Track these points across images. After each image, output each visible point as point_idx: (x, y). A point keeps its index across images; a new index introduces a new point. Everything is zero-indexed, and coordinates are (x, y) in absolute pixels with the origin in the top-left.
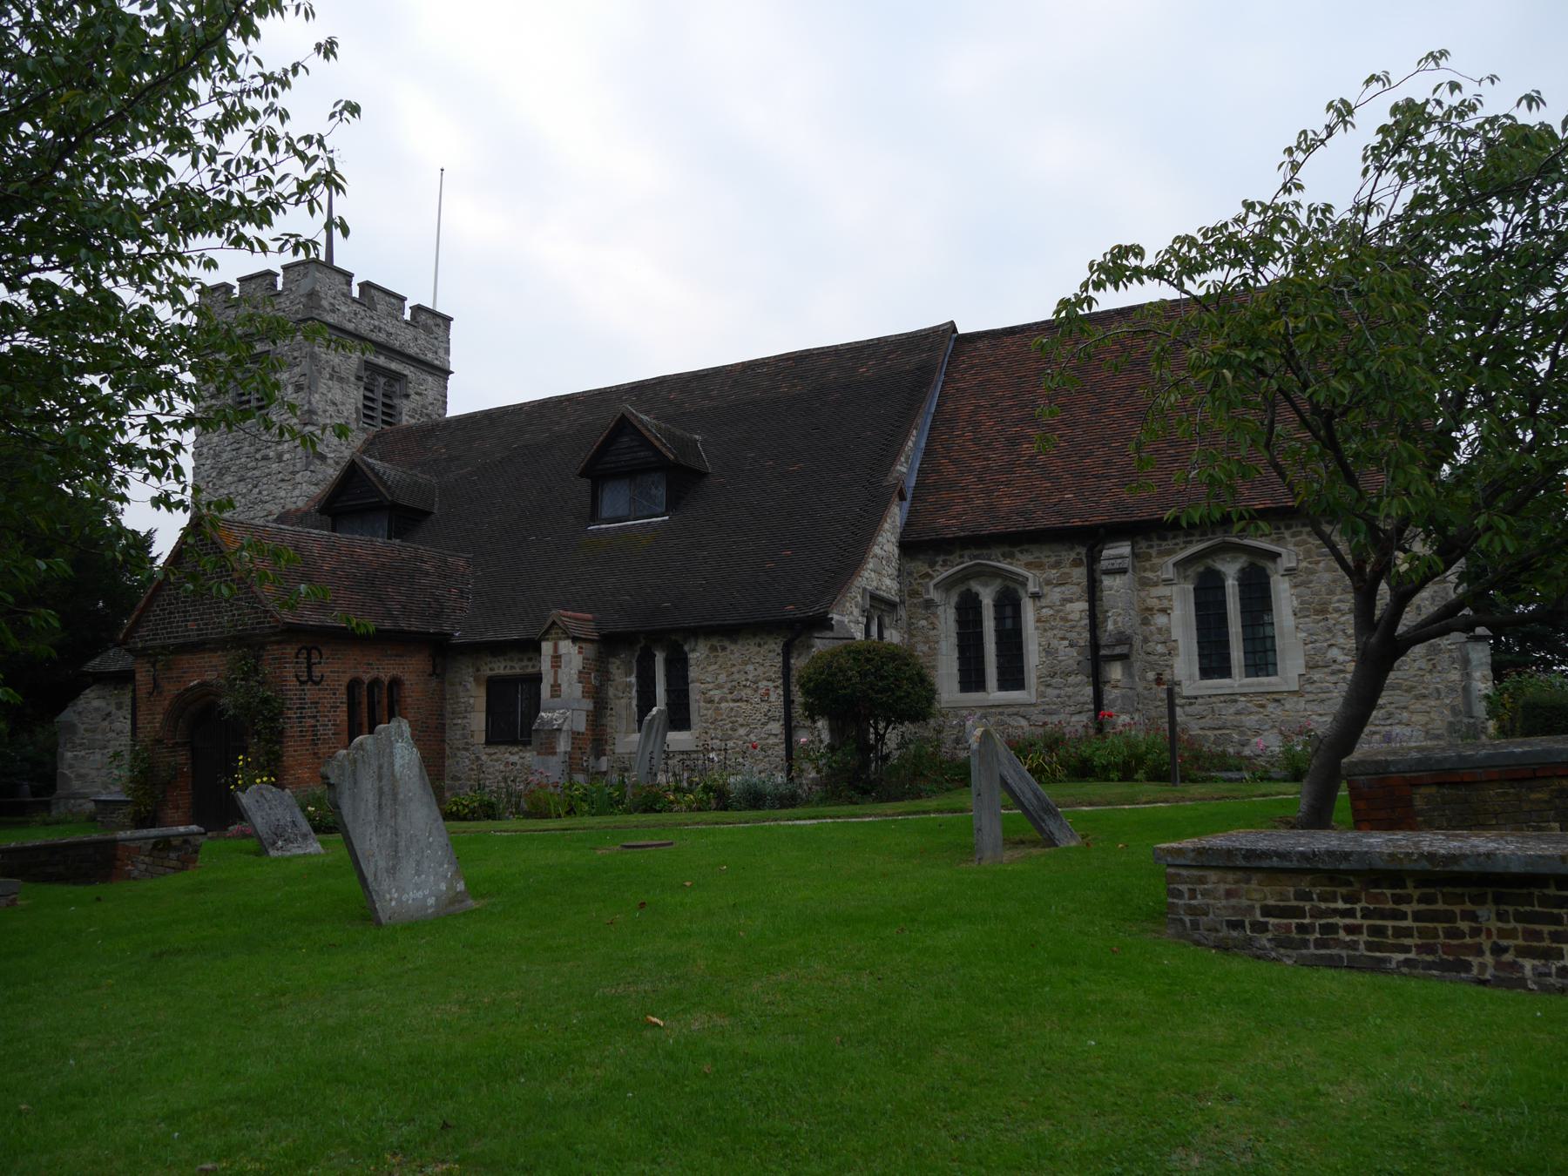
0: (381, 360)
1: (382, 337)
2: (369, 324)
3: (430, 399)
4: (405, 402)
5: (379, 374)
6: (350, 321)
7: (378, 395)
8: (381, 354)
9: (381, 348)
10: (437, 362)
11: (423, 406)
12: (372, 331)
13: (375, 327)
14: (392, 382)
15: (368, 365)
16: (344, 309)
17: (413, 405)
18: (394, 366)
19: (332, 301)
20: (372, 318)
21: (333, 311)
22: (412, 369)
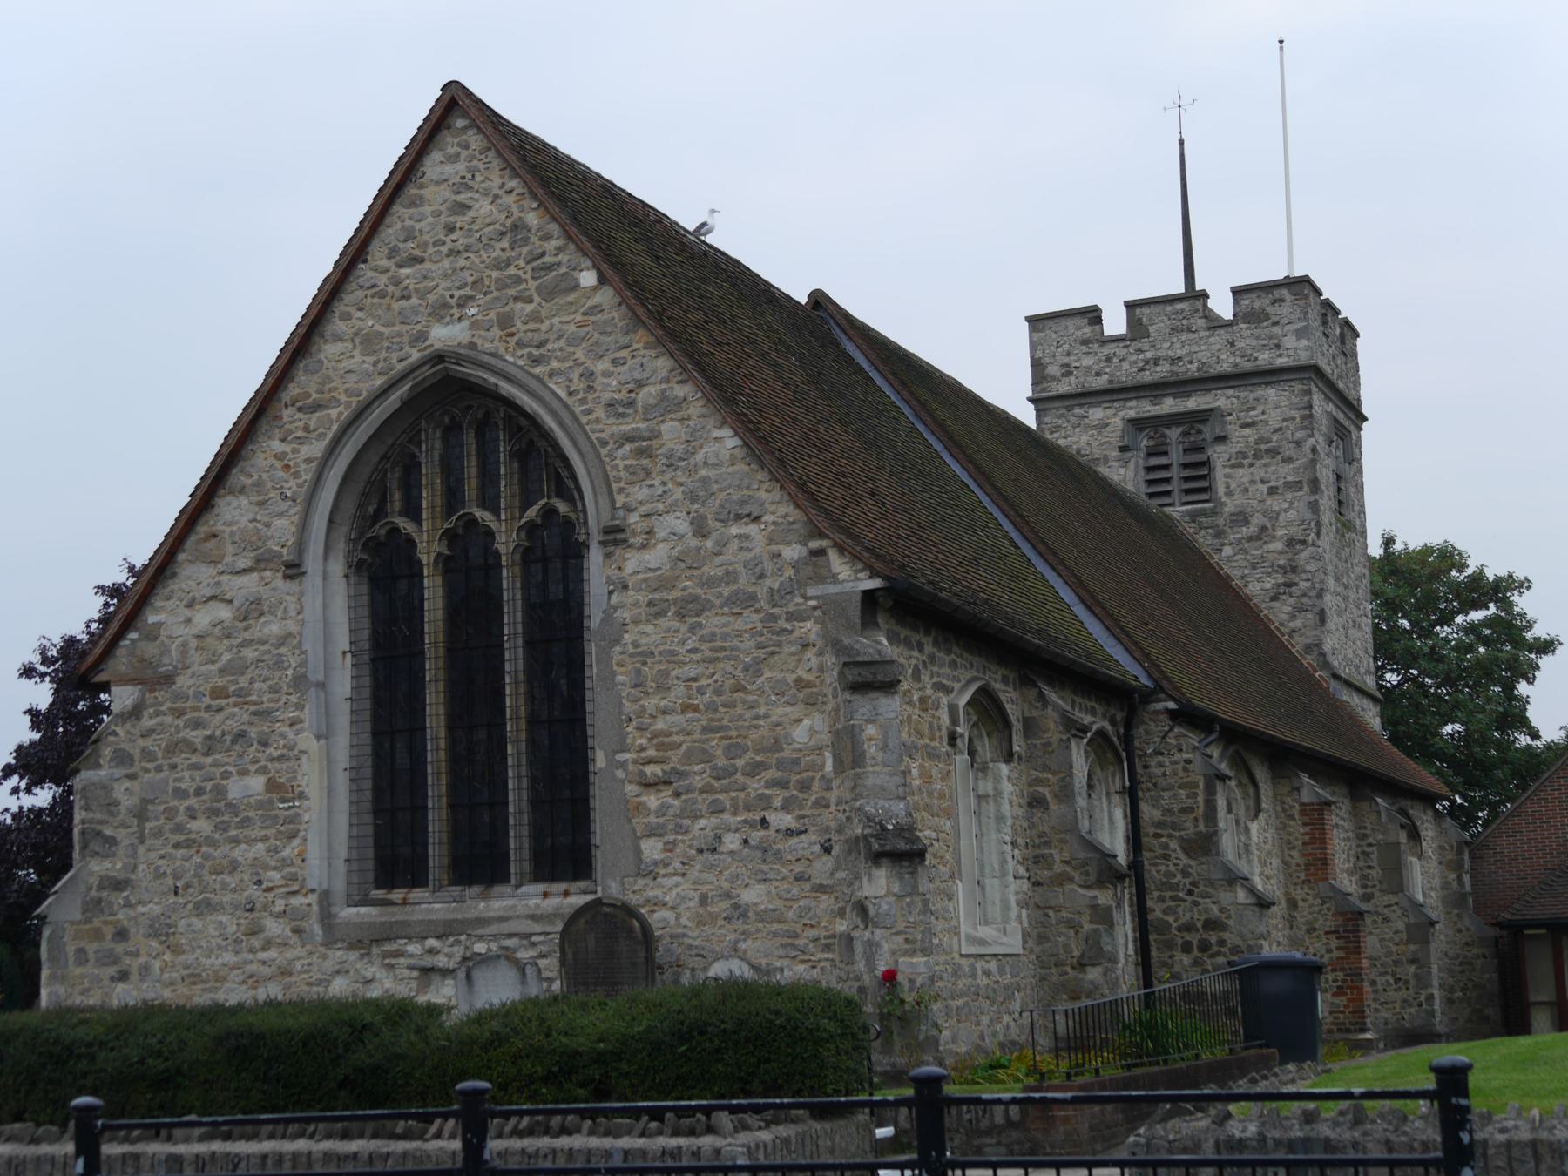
0: (1147, 408)
1: (1162, 371)
2: (1135, 362)
3: (1275, 424)
4: (1220, 448)
5: (1168, 427)
6: (1098, 374)
7: (1176, 456)
8: (1165, 395)
9: (1155, 390)
10: (1281, 362)
11: (1260, 441)
12: (1142, 370)
13: (1147, 362)
14: (1198, 426)
15: (1138, 424)
16: (1087, 361)
17: (1238, 447)
18: (1192, 404)
19: (1066, 360)
20: (1140, 351)
21: (1069, 374)
22: (1230, 392)
